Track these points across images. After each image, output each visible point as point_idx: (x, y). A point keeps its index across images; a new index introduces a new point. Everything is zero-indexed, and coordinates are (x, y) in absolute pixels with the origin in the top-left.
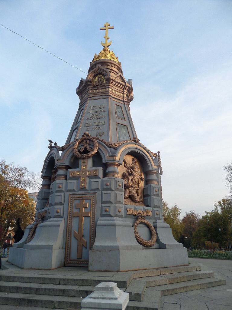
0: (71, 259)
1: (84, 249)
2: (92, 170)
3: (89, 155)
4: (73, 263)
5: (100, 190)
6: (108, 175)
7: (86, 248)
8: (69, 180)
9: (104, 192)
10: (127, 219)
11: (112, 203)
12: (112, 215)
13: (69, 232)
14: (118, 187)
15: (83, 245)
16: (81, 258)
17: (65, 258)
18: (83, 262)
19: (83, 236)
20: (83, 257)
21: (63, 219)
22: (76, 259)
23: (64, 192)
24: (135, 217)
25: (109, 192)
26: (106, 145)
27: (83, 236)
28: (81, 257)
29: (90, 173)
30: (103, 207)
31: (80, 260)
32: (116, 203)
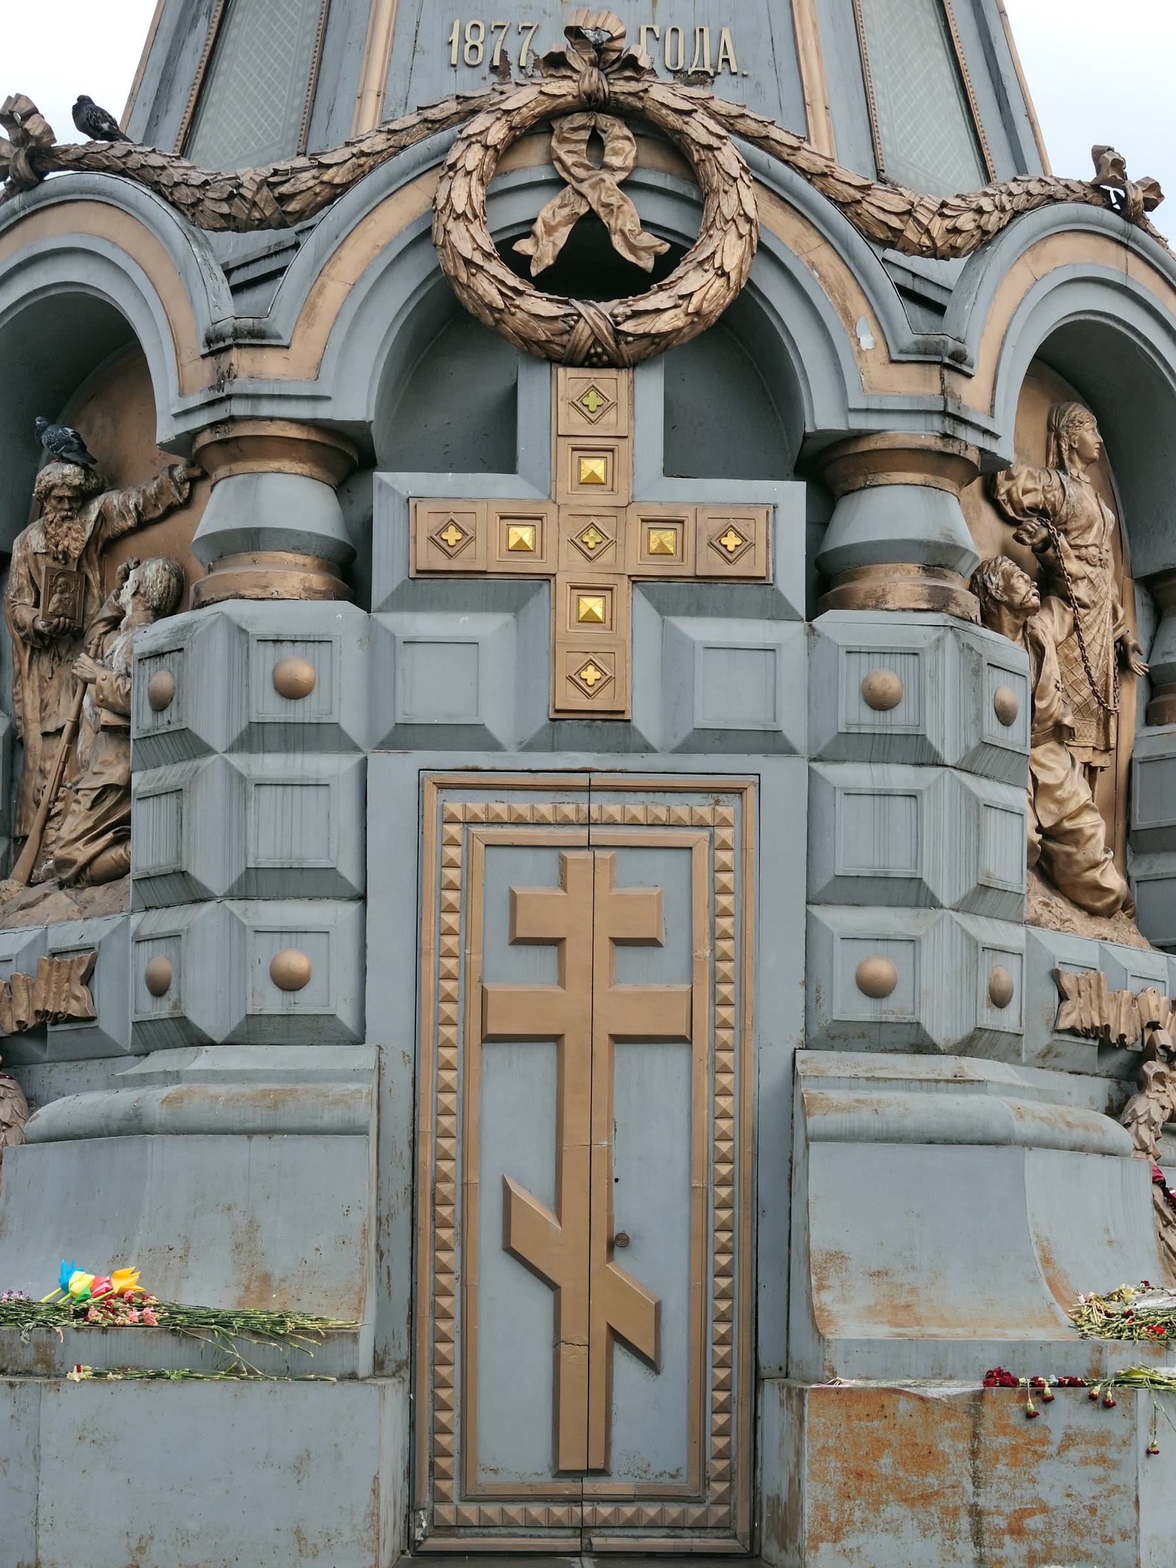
0: (484, 1478)
1: (626, 1368)
2: (699, 507)
3: (663, 323)
4: (509, 1524)
5: (790, 751)
6: (862, 586)
7: (652, 1365)
8: (401, 601)
9: (837, 774)
10: (1060, 1081)
11: (934, 903)
12: (941, 1030)
13: (437, 1200)
14: (993, 729)
15: (615, 1336)
16: (603, 1472)
17: (411, 1473)
18: (628, 1511)
19: (617, 1243)
20: (614, 1466)
21: (362, 1057)
22: (548, 1478)
23: (356, 749)
24: (1121, 1057)
25: (901, 776)
26: (843, 205)
27: (617, 1243)
28: (597, 1463)
29: (667, 537)
30: (838, 945)
31: (591, 1486)
32: (965, 906)
